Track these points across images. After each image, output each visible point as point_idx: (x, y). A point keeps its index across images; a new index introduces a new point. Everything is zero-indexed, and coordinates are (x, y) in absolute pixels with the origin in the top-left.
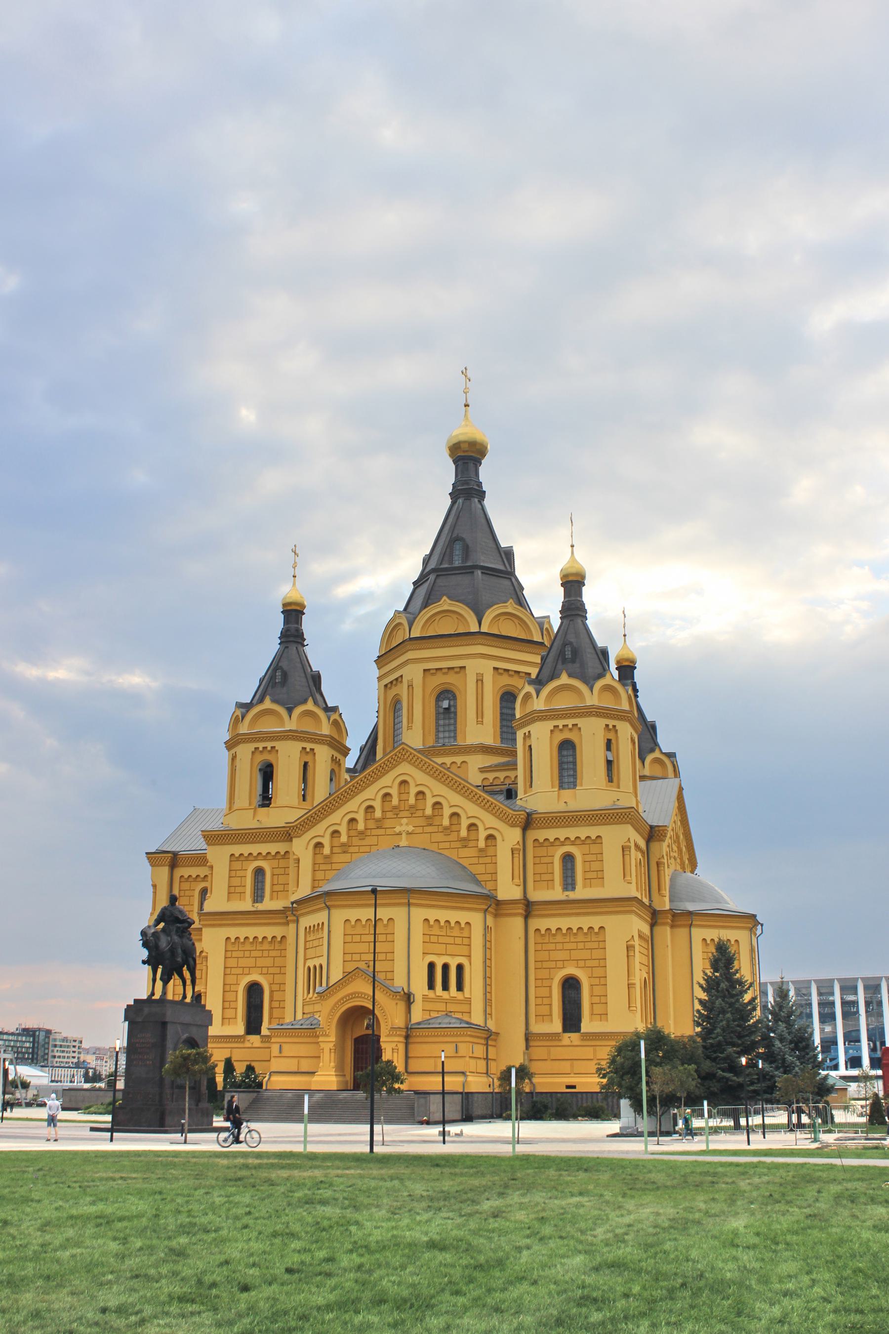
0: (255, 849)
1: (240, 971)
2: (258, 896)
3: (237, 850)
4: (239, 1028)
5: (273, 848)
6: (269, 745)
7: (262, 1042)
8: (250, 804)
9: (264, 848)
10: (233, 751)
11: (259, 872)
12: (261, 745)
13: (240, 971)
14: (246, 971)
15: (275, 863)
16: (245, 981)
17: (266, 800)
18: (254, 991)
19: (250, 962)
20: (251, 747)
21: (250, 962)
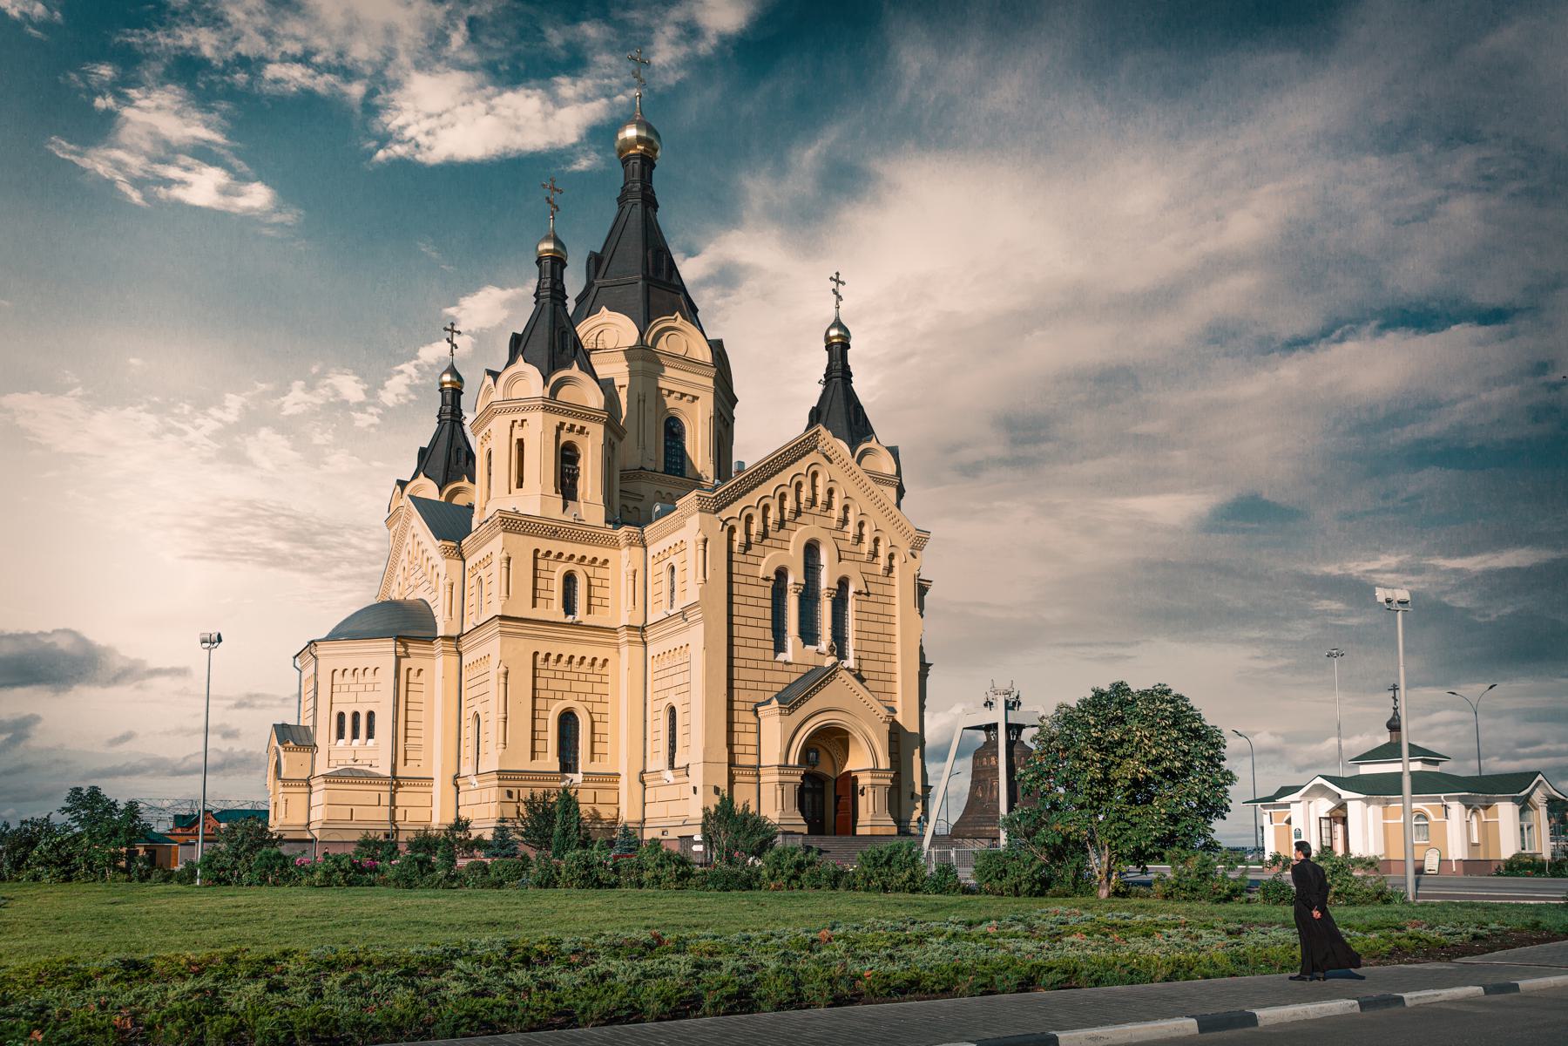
0: (568, 548)
1: (551, 694)
2: (569, 607)
3: (545, 545)
4: (550, 761)
5: (590, 551)
6: (579, 423)
7: (584, 781)
8: (557, 492)
9: (579, 550)
10: (519, 417)
11: (569, 579)
12: (569, 421)
13: (551, 694)
14: (559, 695)
15: (590, 571)
16: (556, 708)
17: (567, 486)
18: (568, 720)
19: (565, 686)
20: (557, 419)
21: (565, 686)
